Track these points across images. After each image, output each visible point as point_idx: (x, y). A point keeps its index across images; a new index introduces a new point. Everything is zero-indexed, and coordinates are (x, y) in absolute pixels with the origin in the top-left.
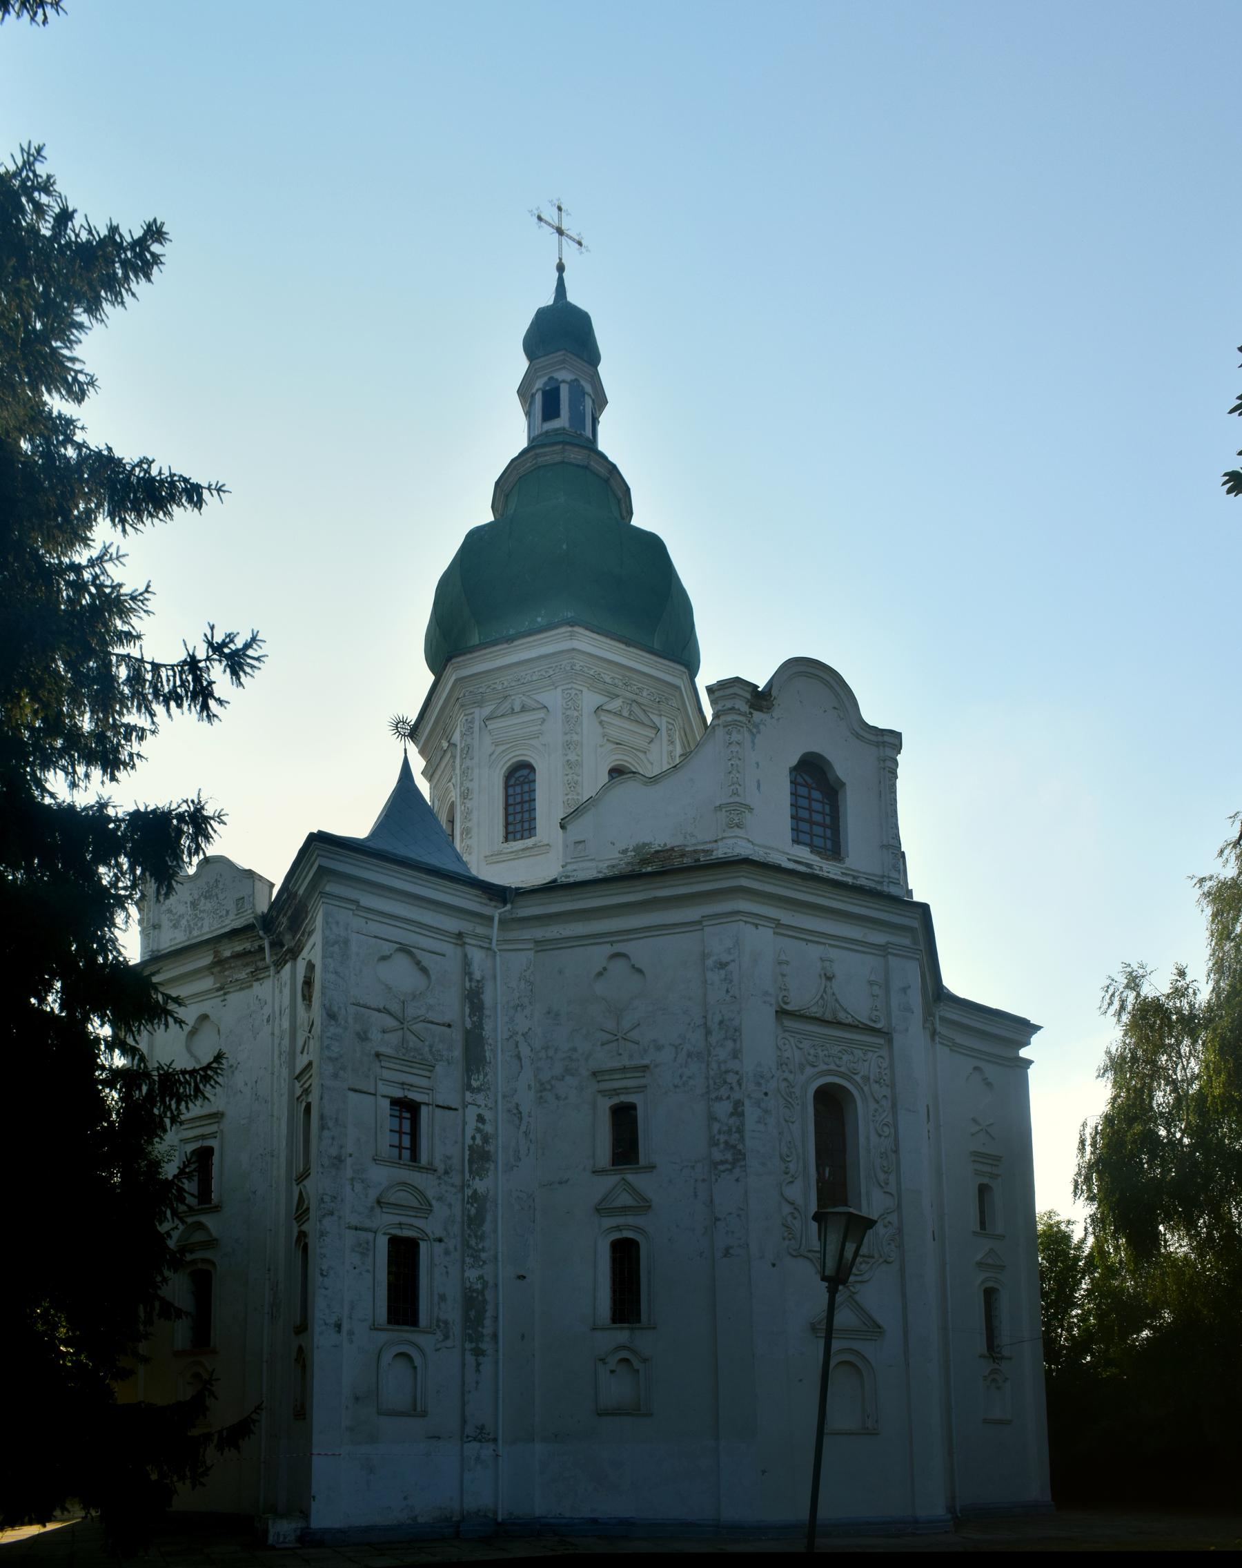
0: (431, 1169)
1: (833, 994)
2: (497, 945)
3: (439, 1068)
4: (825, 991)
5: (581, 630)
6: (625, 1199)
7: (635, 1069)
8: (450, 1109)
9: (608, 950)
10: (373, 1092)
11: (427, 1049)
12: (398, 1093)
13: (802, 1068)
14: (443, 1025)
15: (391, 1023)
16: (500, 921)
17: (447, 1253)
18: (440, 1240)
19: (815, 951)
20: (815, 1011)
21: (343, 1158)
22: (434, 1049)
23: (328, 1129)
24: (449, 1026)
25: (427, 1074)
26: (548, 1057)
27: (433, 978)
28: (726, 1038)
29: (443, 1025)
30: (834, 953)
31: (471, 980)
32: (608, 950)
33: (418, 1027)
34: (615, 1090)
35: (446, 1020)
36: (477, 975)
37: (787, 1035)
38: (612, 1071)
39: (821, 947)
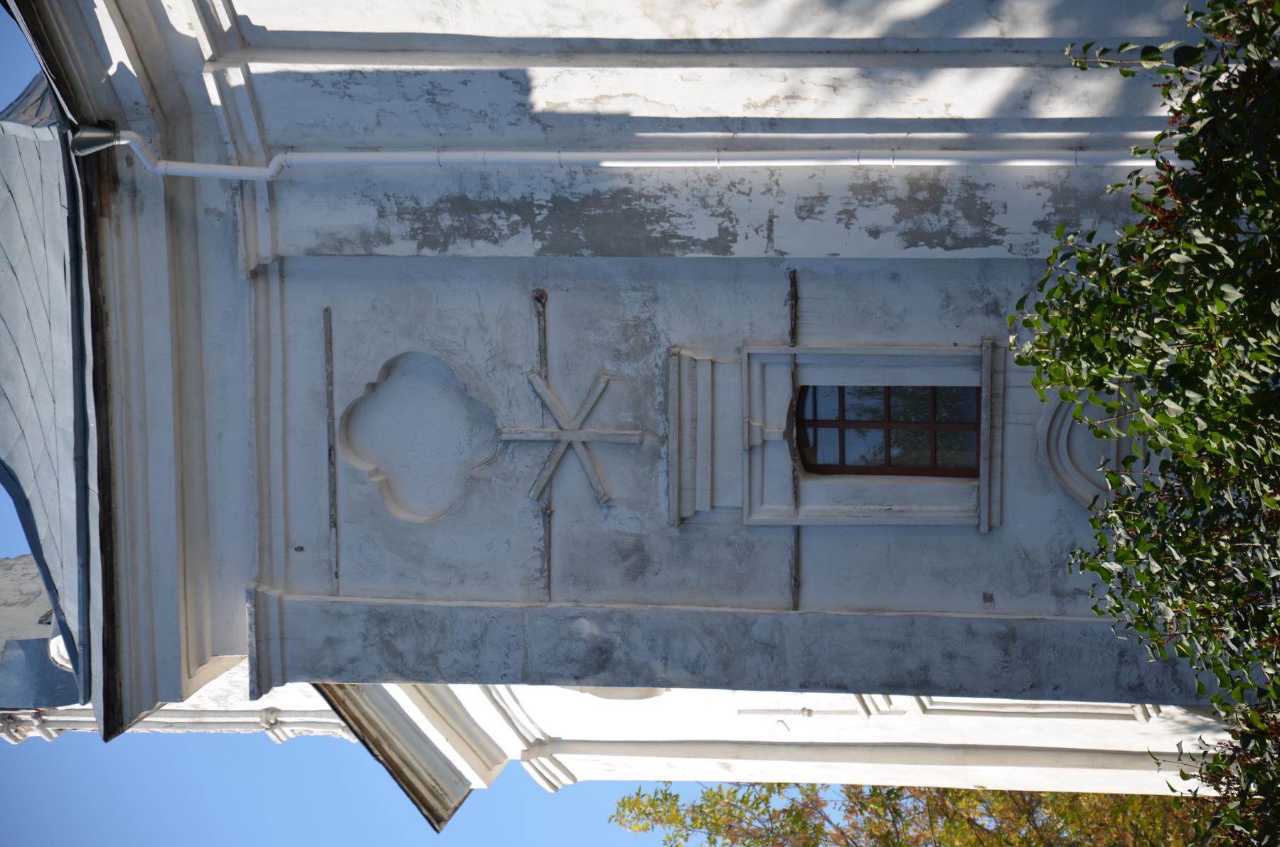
10: (789, 539)
11: (628, 369)
12: (780, 460)
14: (541, 315)
15: (571, 484)
16: (169, 153)
21: (1003, 629)
22: (624, 347)
23: (925, 668)
24: (540, 298)
25: (704, 372)
27: (404, 345)
29: (541, 315)
31: (387, 239)
35: (524, 305)
36: (360, 216)
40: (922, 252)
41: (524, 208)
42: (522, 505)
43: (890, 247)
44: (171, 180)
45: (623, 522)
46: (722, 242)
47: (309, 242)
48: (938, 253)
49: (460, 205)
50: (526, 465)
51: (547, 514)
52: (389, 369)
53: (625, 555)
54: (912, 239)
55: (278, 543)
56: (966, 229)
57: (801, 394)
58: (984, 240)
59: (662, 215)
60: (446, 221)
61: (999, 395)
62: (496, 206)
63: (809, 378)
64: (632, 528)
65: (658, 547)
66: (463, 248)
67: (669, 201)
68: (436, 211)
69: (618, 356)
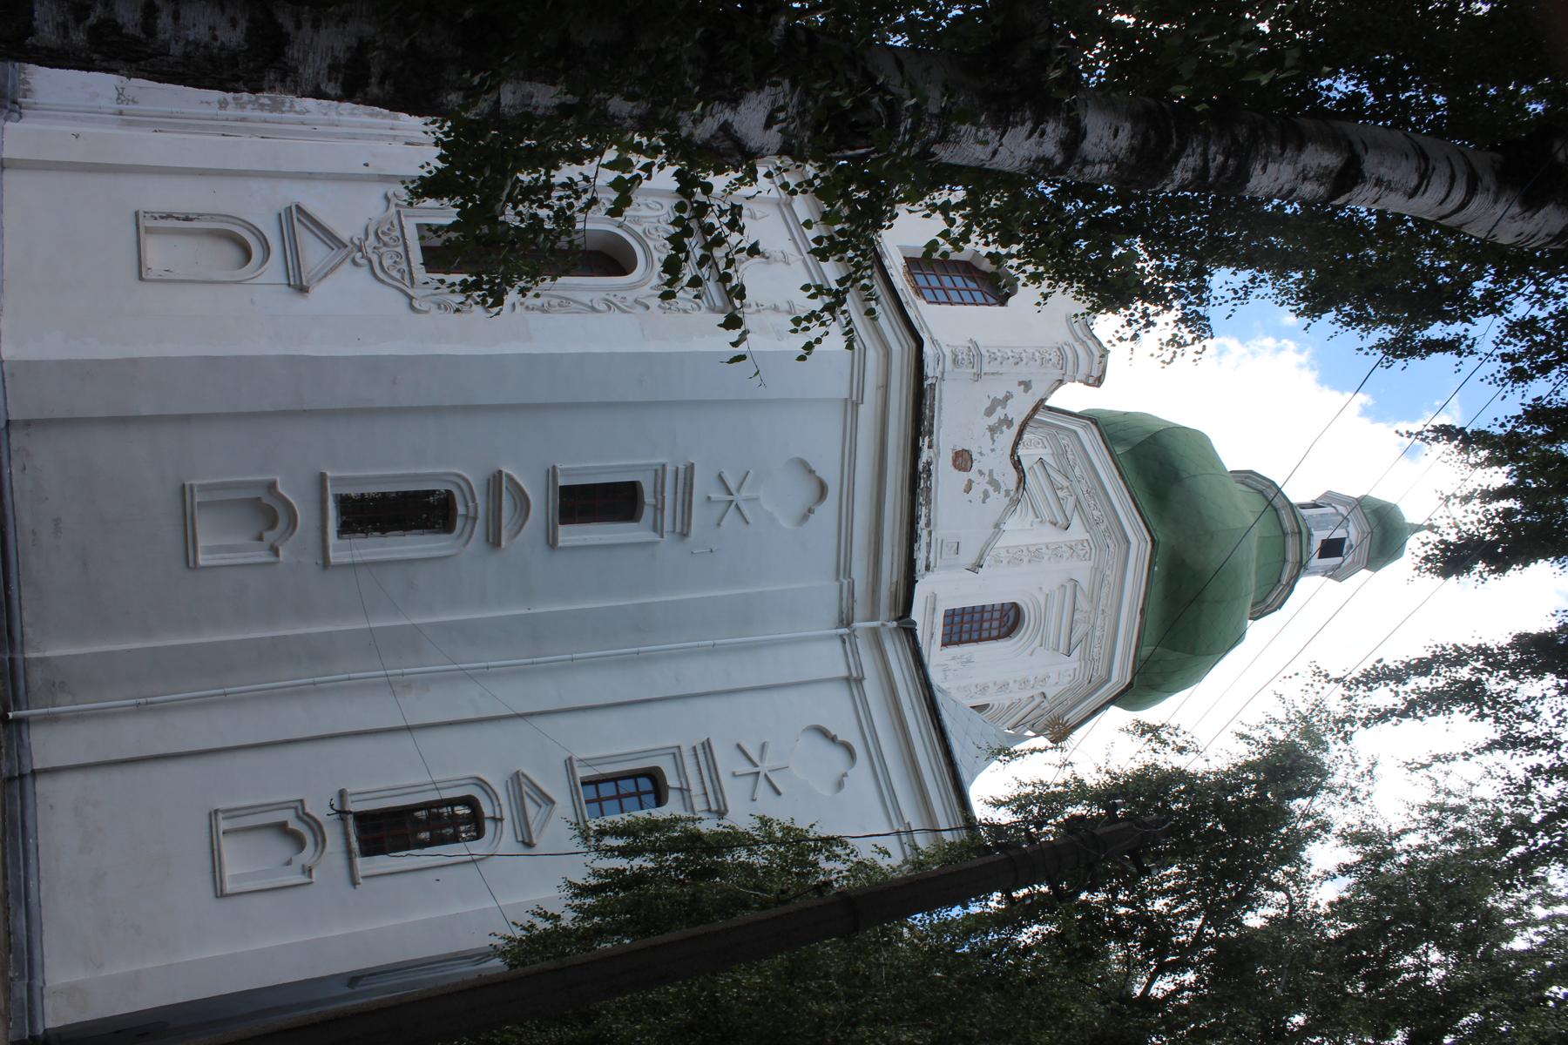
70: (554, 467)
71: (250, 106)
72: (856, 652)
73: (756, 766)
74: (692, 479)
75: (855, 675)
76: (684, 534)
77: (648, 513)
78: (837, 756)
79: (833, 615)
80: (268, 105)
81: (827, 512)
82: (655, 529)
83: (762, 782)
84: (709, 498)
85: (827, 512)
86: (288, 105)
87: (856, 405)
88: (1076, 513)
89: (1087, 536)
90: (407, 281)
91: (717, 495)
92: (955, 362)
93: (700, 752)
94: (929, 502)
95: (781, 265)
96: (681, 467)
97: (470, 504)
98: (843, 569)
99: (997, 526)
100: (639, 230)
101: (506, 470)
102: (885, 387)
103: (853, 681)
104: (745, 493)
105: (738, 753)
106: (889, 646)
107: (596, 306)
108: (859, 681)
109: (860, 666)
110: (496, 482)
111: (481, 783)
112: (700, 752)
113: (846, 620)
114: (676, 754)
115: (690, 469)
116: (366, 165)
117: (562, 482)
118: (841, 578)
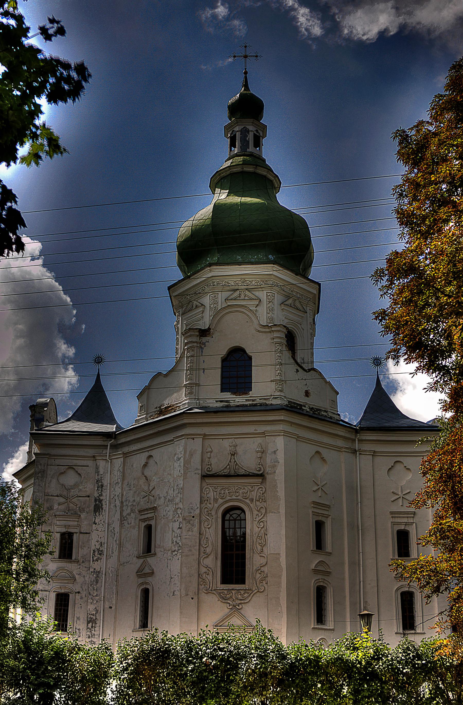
0: (77, 562)
1: (235, 461)
2: (109, 457)
3: (83, 515)
4: (230, 461)
5: (215, 267)
6: (147, 570)
7: (151, 509)
8: (87, 533)
9: (147, 454)
12: (64, 530)
13: (216, 500)
15: (62, 500)
16: (111, 446)
17: (81, 598)
18: (79, 592)
19: (226, 444)
20: (226, 472)
24: (89, 496)
25: (77, 520)
26: (126, 505)
27: (83, 477)
28: (178, 493)
29: (86, 497)
30: (238, 441)
31: (98, 475)
32: (147, 454)
33: (75, 500)
34: (144, 519)
35: (88, 494)
36: (101, 472)
37: (208, 486)
38: (147, 510)
39: (230, 440)
40: (92, 552)
41: (101, 495)
42: (58, 492)
43: (93, 548)
44: (108, 445)
45: (56, 507)
46: (96, 524)
47: (98, 464)
48: (92, 554)
49: (102, 486)
50: (65, 493)
51: (57, 496)
52: (79, 474)
53: (51, 507)
54: (94, 551)
55: (56, 458)
56: (95, 558)
57: (73, 533)
58: (93, 561)
59: (99, 514)
60: (100, 484)
61: (71, 562)
62: (102, 491)
63: (75, 535)
64: (55, 508)
65: (52, 512)
66: (96, 485)
67: (101, 516)
68: (101, 482)
69: (79, 507)
70: (312, 551)
71: (93, 632)
72: (365, 451)
73: (400, 497)
74: (316, 502)
75: (372, 453)
76: (329, 507)
77: (323, 519)
78: (398, 466)
79: (351, 455)
80: (92, 624)
81: (325, 453)
82: (327, 517)
83: (406, 497)
84: (320, 496)
85: (325, 453)
86: (92, 616)
87: (299, 437)
88: (252, 292)
89: (265, 292)
90: (251, 592)
91: (320, 493)
92: (281, 391)
93: (394, 516)
94: (320, 410)
95: (238, 448)
96: (312, 505)
97: (320, 580)
98: (339, 449)
99: (326, 382)
100: (220, 501)
101: (313, 566)
102: (292, 423)
103: (374, 454)
104: (319, 483)
105: (395, 502)
106: (364, 438)
107: (262, 526)
108: (375, 452)
109: (370, 451)
110: (316, 571)
111: (397, 590)
112: (394, 516)
113: (354, 452)
114: (394, 524)
115: (314, 503)
116: (192, 598)
117: (315, 549)
118: (342, 450)
